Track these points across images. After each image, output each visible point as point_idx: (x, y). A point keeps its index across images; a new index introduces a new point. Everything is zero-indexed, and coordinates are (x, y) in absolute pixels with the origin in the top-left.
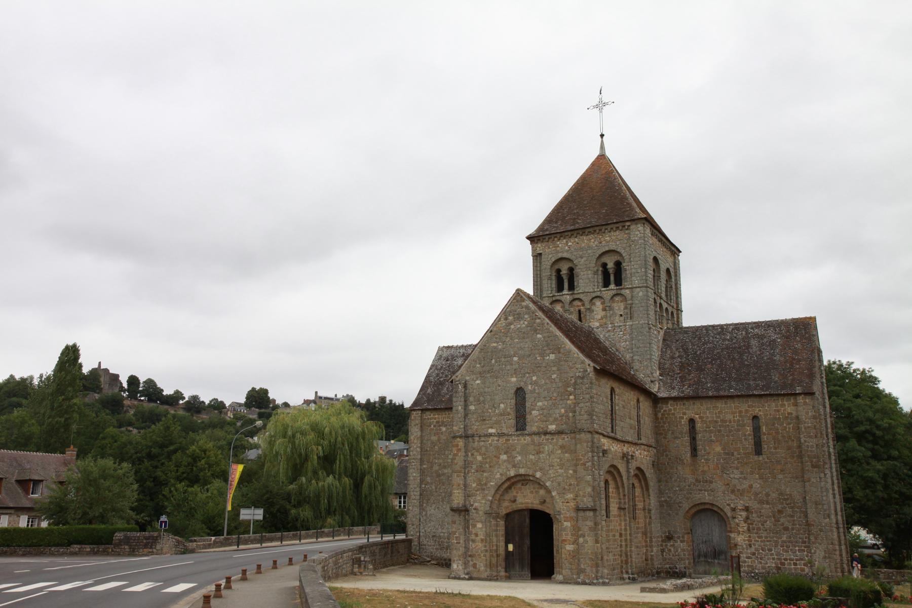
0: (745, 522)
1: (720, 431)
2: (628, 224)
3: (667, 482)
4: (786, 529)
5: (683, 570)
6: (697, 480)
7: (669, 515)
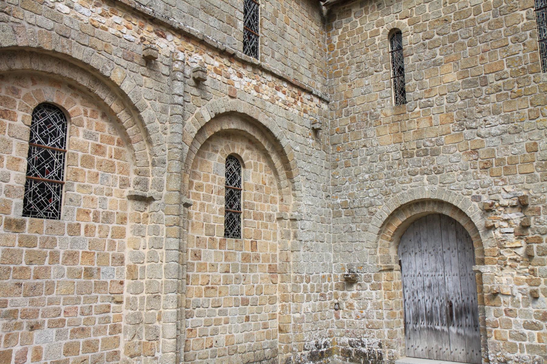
0: (519, 237)
1: (453, 39)
3: (347, 165)
5: (376, 349)
6: (406, 154)
7: (350, 231)
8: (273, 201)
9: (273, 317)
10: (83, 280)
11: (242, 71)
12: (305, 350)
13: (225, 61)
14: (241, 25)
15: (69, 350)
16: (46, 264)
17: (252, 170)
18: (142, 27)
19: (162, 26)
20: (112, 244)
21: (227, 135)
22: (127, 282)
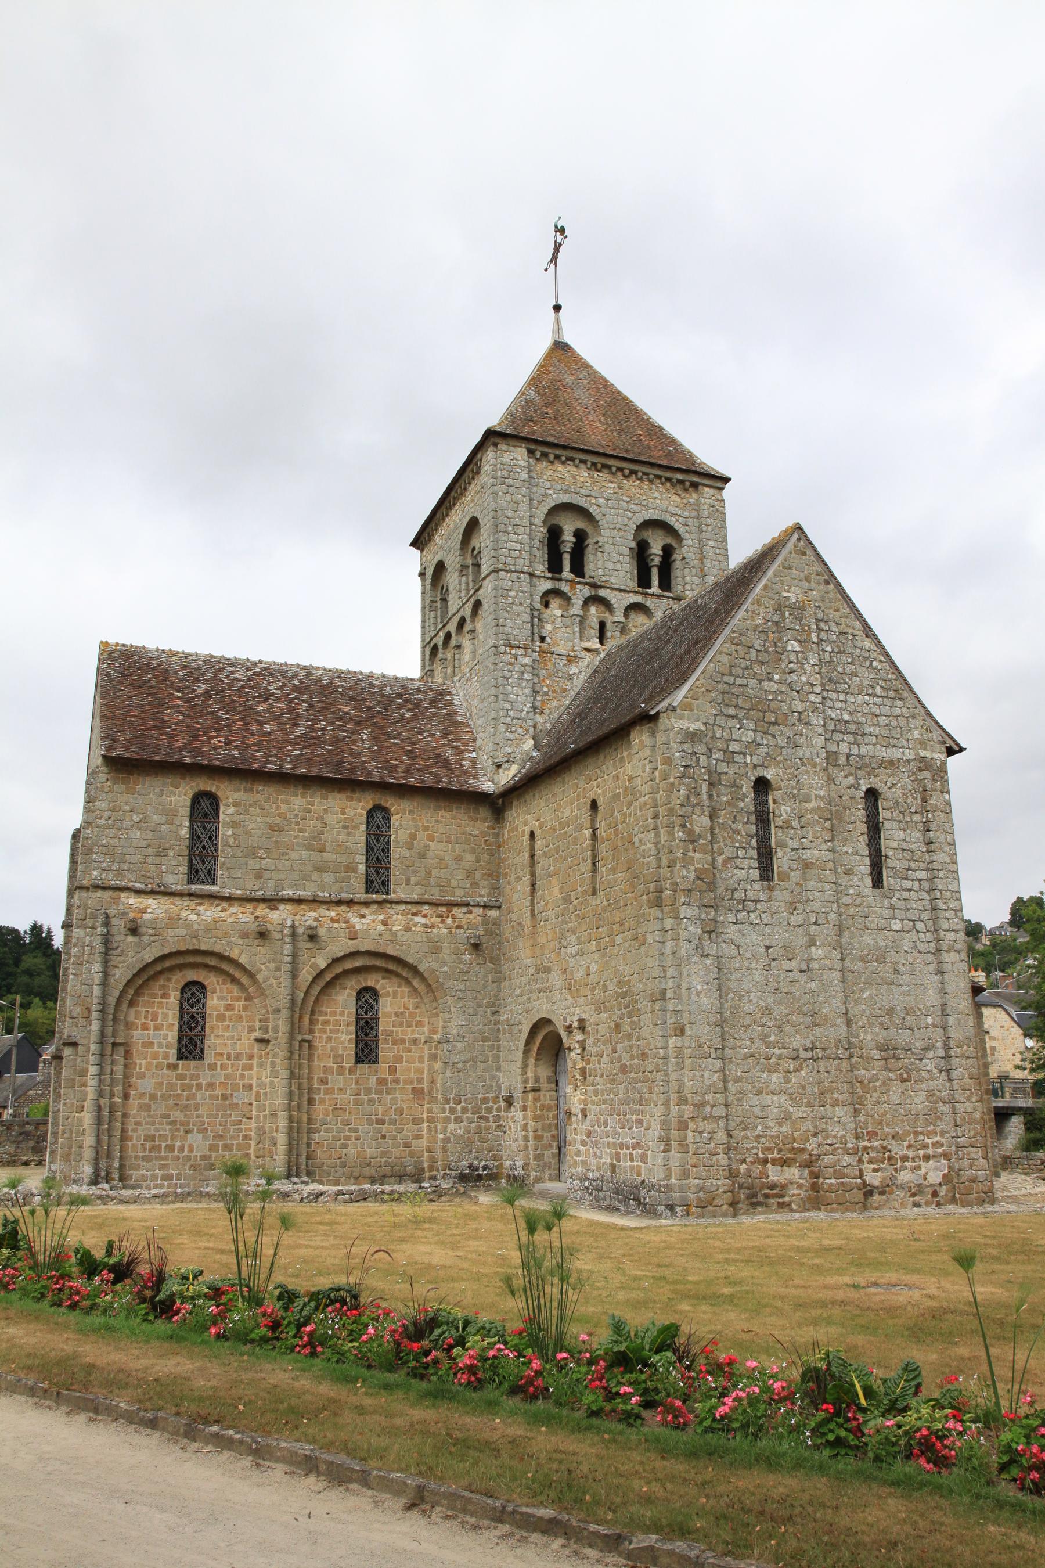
2: (479, 456)
4: (624, 1070)
6: (538, 971)
8: (420, 1024)
9: (418, 1137)
10: (220, 1101)
11: (365, 911)
12: (450, 1169)
13: (343, 908)
14: (362, 868)
15: (212, 1148)
16: (194, 1091)
17: (389, 999)
18: (255, 908)
19: (272, 902)
20: (242, 1077)
21: (358, 971)
22: (254, 1103)
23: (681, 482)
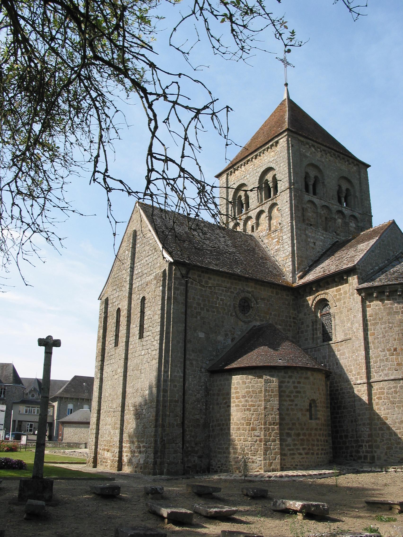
23: (272, 145)
